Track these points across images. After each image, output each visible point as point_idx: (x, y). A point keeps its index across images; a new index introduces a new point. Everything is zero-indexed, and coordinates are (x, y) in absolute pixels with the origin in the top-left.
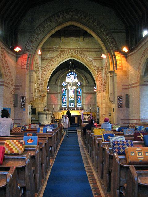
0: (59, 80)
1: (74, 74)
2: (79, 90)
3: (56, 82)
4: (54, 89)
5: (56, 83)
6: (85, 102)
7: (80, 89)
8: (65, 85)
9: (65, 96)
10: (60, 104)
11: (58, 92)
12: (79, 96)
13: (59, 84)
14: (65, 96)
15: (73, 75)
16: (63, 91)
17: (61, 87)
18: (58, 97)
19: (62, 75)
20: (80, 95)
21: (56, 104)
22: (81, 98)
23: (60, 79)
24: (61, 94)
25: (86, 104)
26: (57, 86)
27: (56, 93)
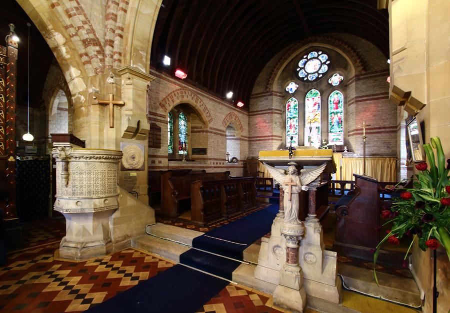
0: (273, 79)
1: (319, 55)
2: (336, 96)
3: (268, 84)
4: (263, 102)
5: (267, 88)
6: (353, 128)
7: (337, 94)
8: (294, 89)
9: (294, 118)
10: (281, 140)
11: (272, 109)
12: (337, 113)
13: (275, 87)
14: (294, 118)
15: (317, 58)
16: (289, 106)
17: (283, 97)
18: (272, 122)
19: (281, 65)
20: (339, 110)
21: (269, 140)
22: (340, 119)
23: (276, 74)
24: (282, 112)
25: (356, 134)
26: (271, 95)
27: (269, 113)
